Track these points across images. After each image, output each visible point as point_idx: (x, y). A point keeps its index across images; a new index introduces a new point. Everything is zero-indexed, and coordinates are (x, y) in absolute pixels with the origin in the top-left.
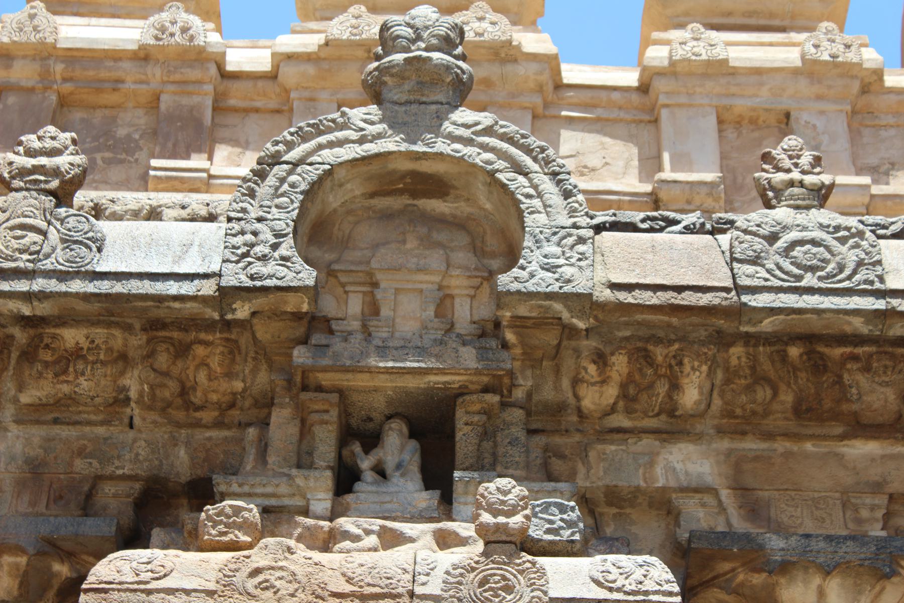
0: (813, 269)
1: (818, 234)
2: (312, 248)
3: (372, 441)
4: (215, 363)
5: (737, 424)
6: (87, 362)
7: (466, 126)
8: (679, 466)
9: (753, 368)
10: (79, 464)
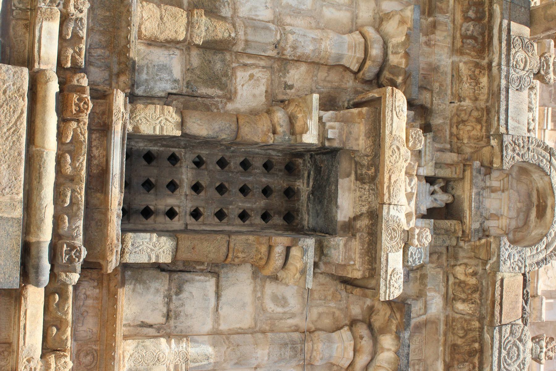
0: (508, 354)
1: (522, 357)
2: (517, 168)
3: (445, 189)
4: (474, 132)
5: (450, 323)
8: (434, 301)
9: (470, 330)
10: (437, 84)
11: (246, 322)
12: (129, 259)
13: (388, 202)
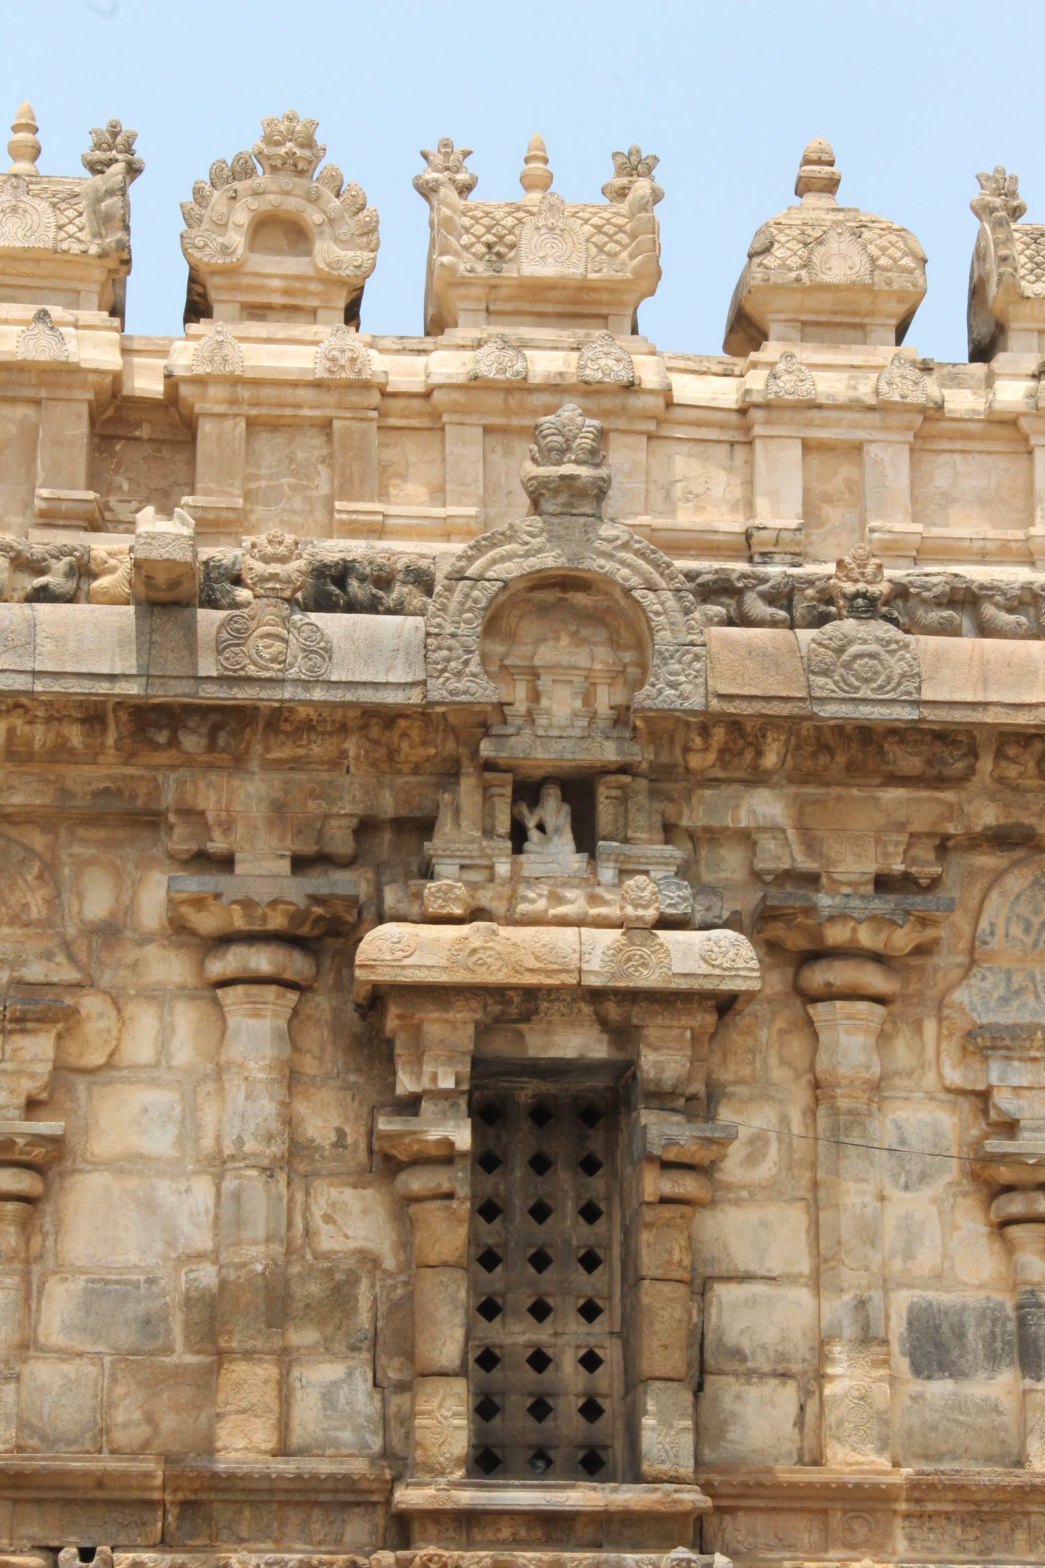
0: (867, 681)
1: (874, 648)
2: (488, 642)
4: (415, 734)
5: (801, 778)
6: (318, 734)
7: (609, 541)
8: (758, 809)
9: (818, 739)
10: (312, 805)
11: (797, 1218)
12: (686, 1467)
13: (576, 975)
